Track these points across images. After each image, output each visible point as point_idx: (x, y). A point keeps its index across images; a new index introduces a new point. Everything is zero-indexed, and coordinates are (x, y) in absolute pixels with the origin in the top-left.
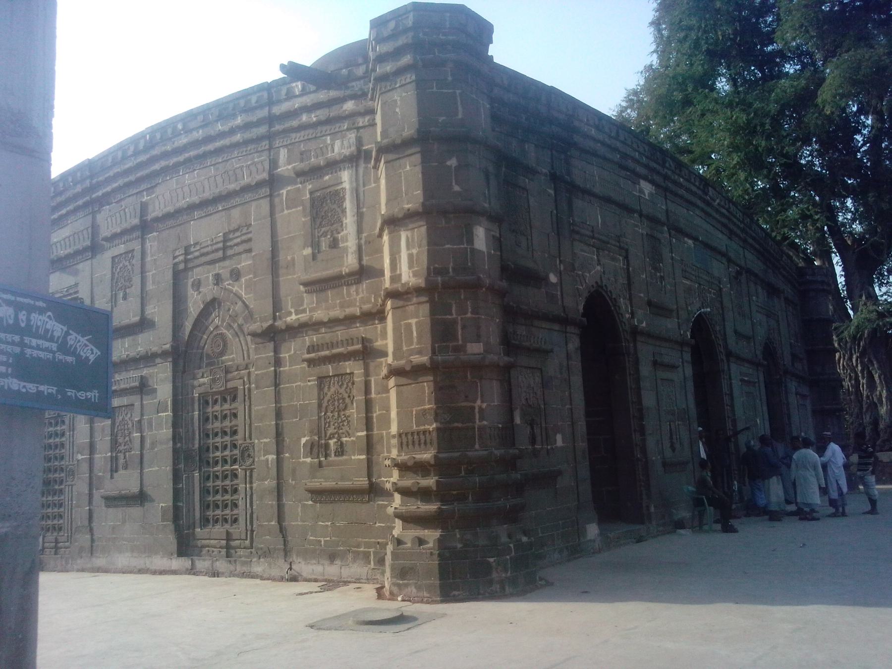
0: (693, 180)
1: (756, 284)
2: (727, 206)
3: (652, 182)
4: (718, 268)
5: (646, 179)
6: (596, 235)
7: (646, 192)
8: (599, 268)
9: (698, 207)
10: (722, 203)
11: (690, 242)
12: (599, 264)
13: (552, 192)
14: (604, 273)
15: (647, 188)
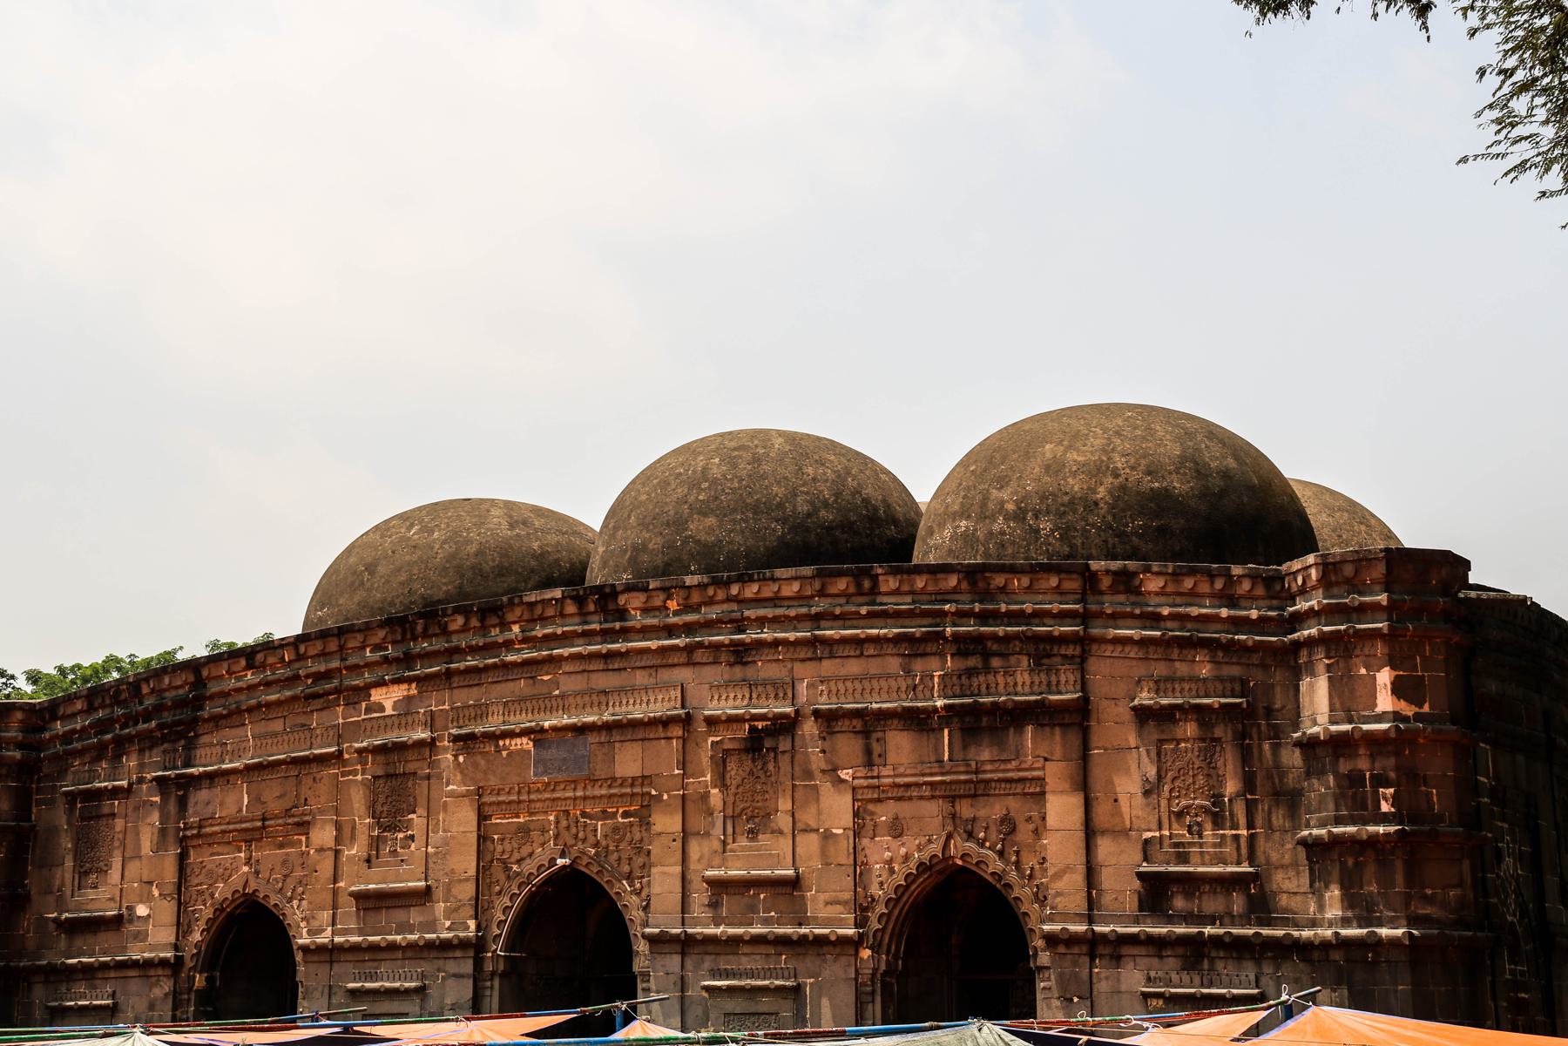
0: (550, 612)
1: (866, 734)
2: (721, 595)
3: (397, 681)
4: (629, 761)
5: (381, 683)
6: (231, 827)
7: (388, 705)
8: (246, 869)
9: (560, 660)
10: (696, 598)
11: (525, 743)
12: (248, 862)
13: (157, 799)
14: (257, 873)
15: (388, 698)
